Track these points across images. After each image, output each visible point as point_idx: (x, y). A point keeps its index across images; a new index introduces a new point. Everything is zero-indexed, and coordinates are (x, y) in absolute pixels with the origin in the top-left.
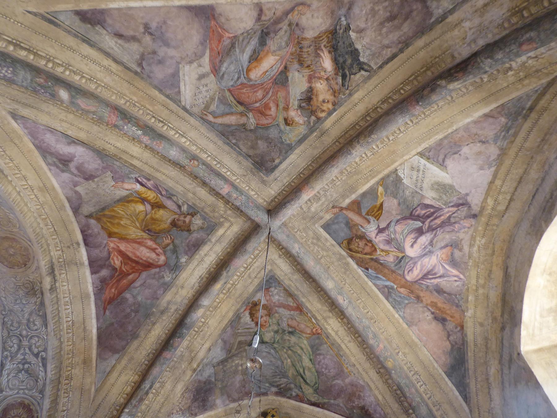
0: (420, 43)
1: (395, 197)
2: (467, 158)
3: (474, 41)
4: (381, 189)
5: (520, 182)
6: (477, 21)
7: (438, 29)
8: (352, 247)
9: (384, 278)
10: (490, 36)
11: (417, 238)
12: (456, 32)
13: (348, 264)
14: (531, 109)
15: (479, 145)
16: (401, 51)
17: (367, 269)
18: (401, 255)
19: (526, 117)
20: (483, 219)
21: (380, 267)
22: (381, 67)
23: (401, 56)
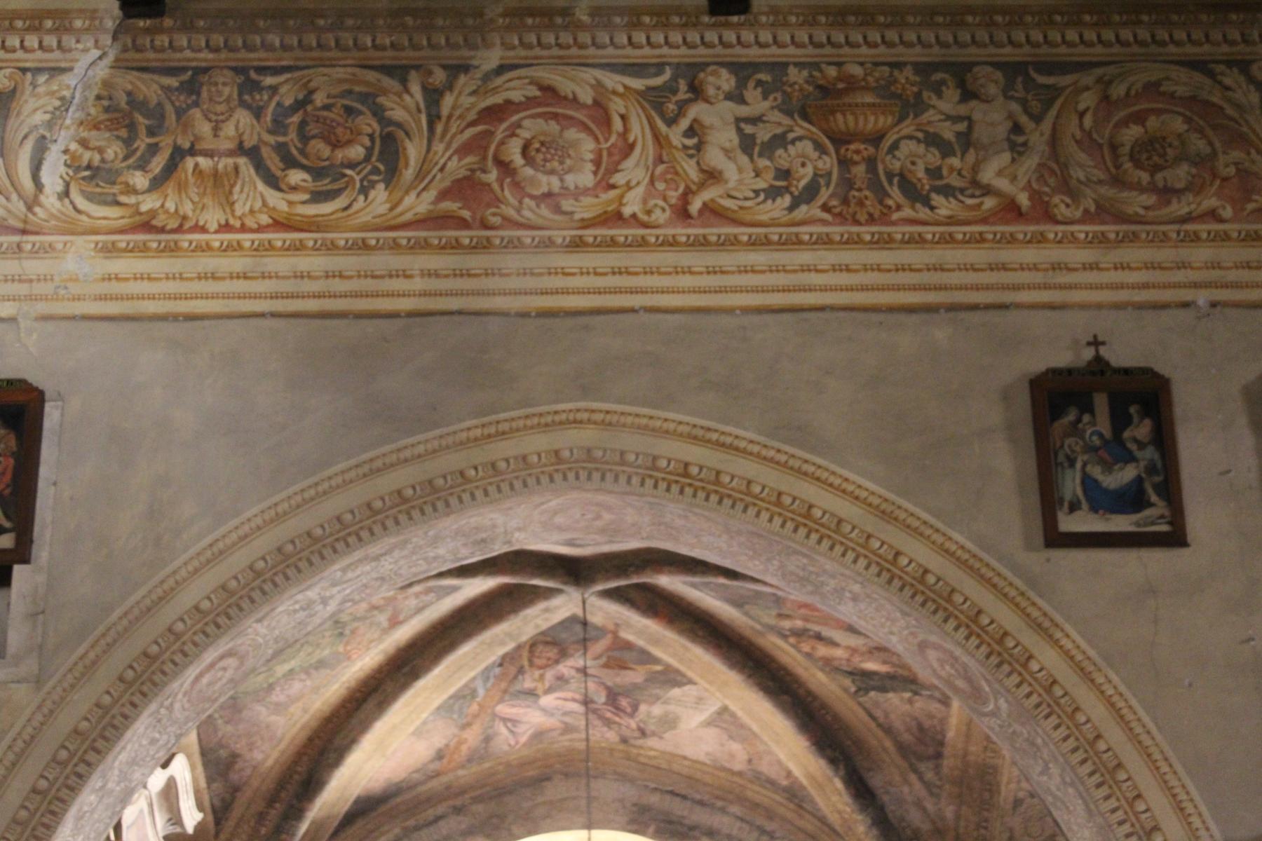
0: (888, 744)
1: (646, 680)
2: (722, 745)
3: (887, 793)
4: (659, 668)
5: (689, 778)
6: (909, 799)
7: (905, 765)
8: (540, 648)
9: (489, 685)
10: (893, 808)
11: (574, 700)
12: (897, 778)
13: (503, 643)
14: (801, 807)
15: (746, 757)
16: (879, 725)
17: (501, 665)
18: (539, 692)
19: (789, 799)
20: (621, 747)
21: (511, 676)
22: (860, 704)
23: (873, 725)
